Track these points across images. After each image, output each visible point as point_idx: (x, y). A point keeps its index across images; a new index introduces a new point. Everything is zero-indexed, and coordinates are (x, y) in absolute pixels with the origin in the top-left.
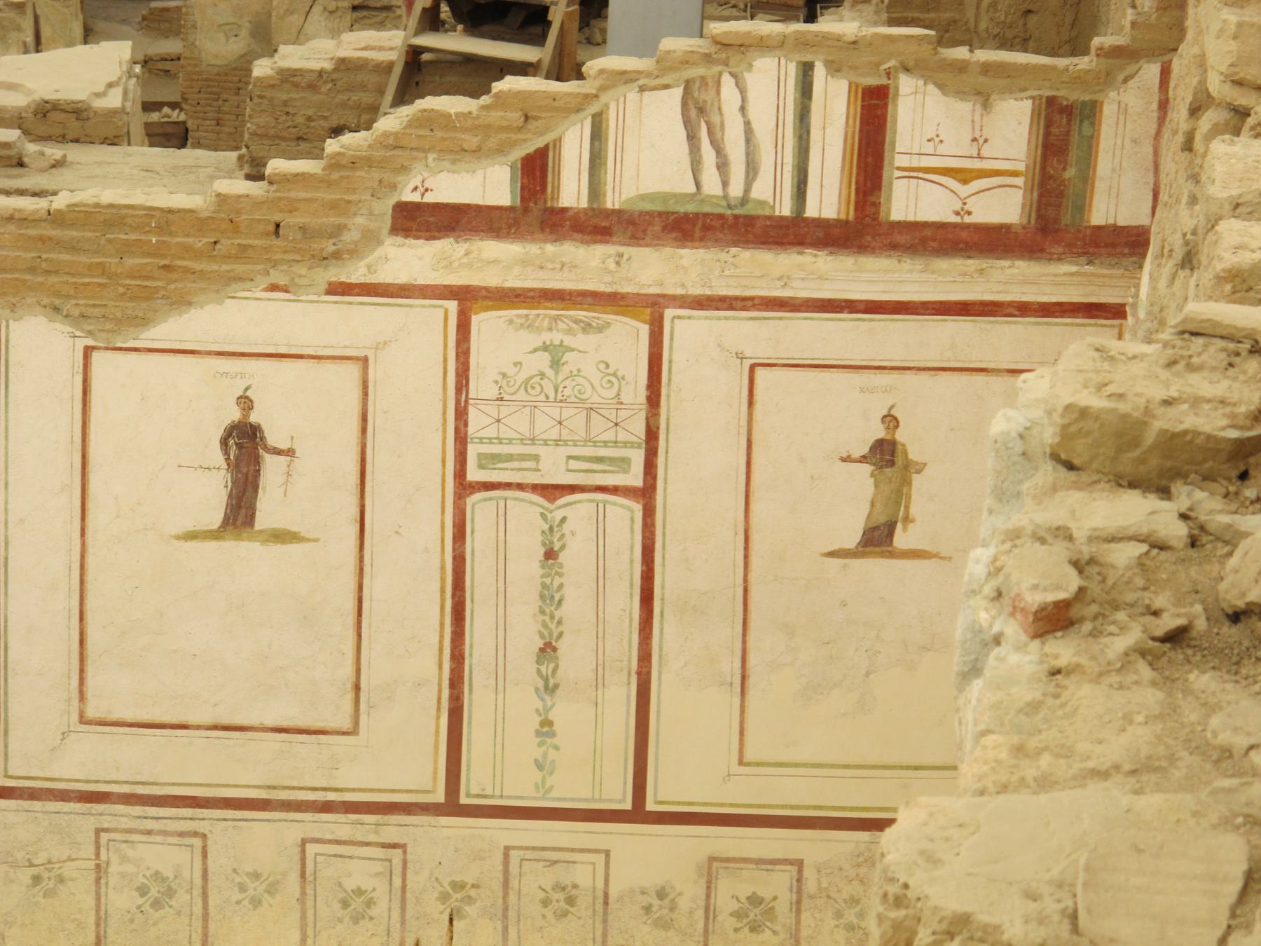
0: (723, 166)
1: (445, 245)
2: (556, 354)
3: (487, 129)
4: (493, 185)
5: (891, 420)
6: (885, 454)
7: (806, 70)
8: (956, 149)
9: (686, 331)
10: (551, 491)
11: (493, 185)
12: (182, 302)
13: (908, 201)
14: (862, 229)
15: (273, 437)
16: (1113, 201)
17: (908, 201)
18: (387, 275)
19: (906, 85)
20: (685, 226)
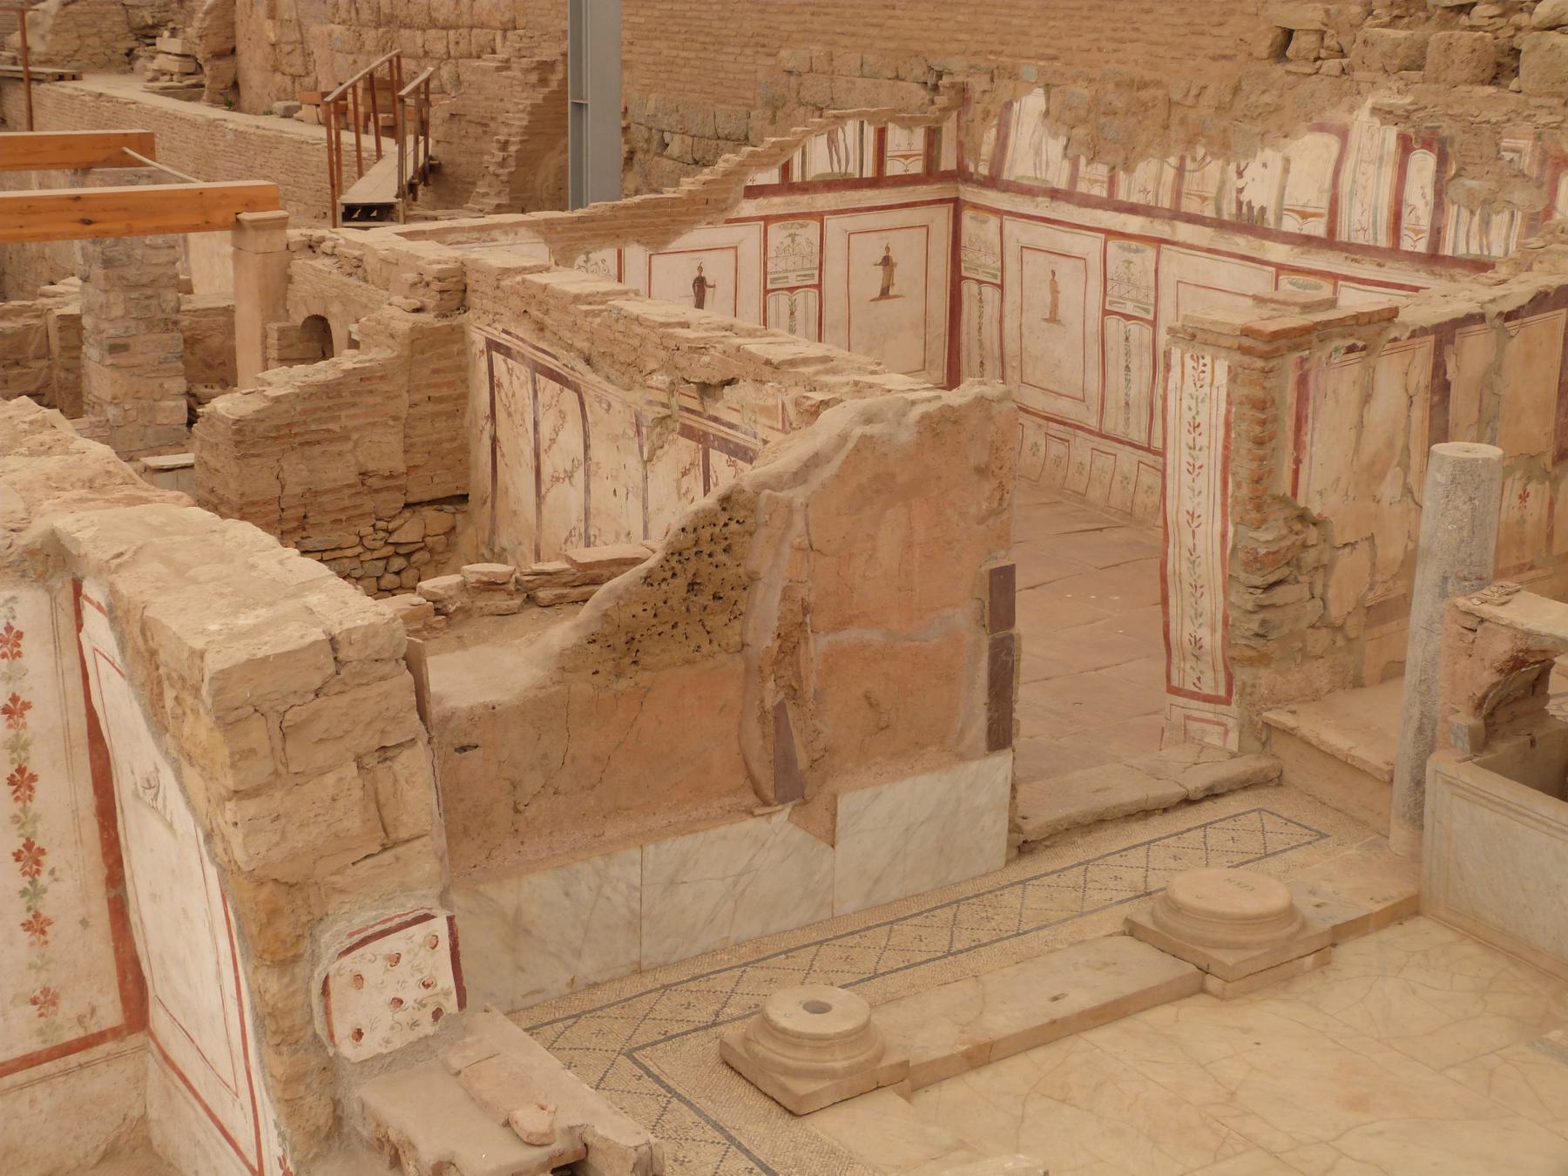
0: (839, 161)
1: (761, 201)
2: (793, 236)
3: (770, 156)
4: (771, 177)
5: (888, 249)
6: (887, 262)
7: (862, 123)
9: (832, 223)
10: (791, 289)
11: (771, 177)
13: (894, 168)
14: (879, 181)
15: (709, 282)
16: (948, 162)
17: (894, 168)
18: (744, 214)
19: (890, 126)
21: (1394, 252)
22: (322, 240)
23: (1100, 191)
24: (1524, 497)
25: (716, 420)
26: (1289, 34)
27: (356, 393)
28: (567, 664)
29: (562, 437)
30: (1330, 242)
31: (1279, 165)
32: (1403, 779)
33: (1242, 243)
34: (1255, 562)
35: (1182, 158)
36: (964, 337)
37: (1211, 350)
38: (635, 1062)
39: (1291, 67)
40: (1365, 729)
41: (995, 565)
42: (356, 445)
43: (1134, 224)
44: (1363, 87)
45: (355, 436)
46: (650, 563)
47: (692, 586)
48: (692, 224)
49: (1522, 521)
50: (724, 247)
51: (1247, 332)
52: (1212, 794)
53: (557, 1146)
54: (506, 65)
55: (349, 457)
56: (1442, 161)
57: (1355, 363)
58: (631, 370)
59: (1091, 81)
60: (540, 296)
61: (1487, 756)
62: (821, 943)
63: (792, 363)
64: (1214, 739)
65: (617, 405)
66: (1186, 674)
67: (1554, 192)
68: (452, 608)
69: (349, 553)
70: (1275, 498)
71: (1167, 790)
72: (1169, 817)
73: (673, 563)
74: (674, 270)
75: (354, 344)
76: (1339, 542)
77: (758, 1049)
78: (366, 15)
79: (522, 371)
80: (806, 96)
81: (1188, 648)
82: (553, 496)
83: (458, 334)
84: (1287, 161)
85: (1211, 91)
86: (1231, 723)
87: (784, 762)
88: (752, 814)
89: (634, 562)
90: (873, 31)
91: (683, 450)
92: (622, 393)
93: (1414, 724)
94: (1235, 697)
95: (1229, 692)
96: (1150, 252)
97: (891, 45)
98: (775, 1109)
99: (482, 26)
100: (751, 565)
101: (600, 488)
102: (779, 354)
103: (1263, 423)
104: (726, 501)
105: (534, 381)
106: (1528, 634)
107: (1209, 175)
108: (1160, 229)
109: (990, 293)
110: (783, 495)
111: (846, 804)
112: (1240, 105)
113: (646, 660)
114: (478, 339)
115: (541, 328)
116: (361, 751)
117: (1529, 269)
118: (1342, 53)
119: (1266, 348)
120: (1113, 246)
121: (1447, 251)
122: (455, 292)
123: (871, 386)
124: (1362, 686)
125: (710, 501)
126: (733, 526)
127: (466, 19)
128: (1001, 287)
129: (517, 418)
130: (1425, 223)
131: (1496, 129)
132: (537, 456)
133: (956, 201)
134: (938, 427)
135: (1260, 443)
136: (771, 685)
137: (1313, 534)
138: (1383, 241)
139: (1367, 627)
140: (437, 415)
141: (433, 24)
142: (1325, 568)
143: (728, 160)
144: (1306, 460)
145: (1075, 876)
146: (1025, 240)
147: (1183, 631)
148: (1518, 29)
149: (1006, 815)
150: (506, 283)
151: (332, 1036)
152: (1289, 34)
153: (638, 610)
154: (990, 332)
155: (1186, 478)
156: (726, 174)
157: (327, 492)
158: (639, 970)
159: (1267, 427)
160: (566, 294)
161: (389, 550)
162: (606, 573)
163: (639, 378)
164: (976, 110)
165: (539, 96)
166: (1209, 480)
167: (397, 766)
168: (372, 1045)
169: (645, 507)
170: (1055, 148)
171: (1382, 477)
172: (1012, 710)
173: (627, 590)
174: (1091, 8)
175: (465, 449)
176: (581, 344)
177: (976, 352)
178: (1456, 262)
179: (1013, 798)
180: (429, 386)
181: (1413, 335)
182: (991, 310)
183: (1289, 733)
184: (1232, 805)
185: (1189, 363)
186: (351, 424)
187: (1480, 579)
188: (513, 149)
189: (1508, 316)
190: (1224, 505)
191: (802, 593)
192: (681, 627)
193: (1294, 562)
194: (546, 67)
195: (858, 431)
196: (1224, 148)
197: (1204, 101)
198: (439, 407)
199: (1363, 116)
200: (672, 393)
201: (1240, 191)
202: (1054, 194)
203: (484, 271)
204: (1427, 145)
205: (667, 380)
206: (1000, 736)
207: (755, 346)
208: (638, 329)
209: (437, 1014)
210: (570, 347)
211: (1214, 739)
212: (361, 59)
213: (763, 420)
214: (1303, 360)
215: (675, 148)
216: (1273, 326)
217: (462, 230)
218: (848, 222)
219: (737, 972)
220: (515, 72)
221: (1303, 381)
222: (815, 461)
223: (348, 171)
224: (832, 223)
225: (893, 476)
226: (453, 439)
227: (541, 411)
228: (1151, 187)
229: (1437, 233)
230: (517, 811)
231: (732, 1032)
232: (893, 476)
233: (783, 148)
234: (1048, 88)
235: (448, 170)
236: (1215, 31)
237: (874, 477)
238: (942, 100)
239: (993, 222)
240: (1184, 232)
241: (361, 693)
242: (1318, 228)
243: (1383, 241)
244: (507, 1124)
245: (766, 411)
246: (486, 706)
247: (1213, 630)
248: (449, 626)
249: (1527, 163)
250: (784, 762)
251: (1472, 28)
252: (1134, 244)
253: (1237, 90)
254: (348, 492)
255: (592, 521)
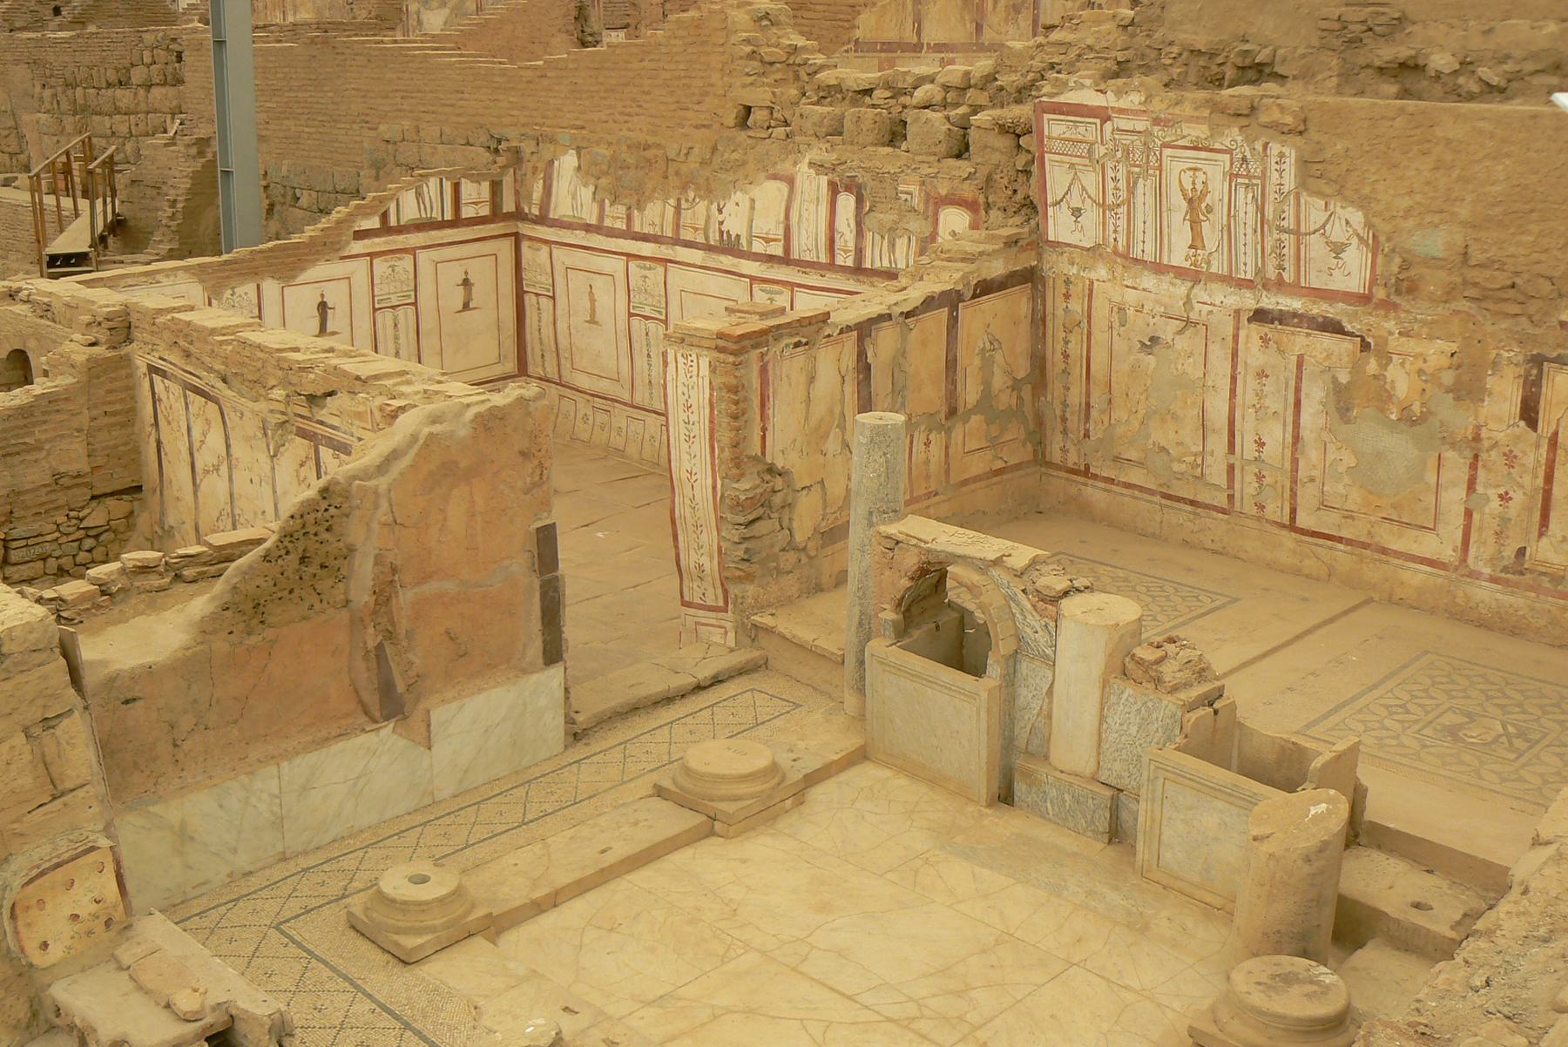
4: (373, 223)
6: (466, 283)
8: (474, 197)
9: (422, 256)
11: (373, 223)
12: (304, 269)
13: (467, 212)
14: (457, 222)
16: (508, 206)
17: (467, 212)
20: (419, 226)
21: (831, 266)
22: (19, 290)
23: (621, 225)
24: (927, 444)
25: (322, 423)
26: (748, 109)
27: (44, 413)
28: (206, 629)
29: (209, 439)
30: (786, 260)
31: (747, 204)
32: (851, 661)
33: (727, 261)
34: (738, 506)
35: (679, 200)
36: (528, 337)
37: (697, 350)
38: (282, 933)
39: (751, 133)
40: (824, 623)
41: (540, 524)
42: (49, 454)
43: (647, 249)
44: (802, 147)
45: (47, 447)
46: (267, 545)
47: (303, 560)
48: (314, 262)
49: (927, 461)
50: (340, 279)
51: (721, 336)
52: (717, 681)
53: (209, 1020)
54: (172, 142)
55: (44, 463)
56: (860, 201)
57: (800, 359)
58: (258, 387)
59: (610, 144)
60: (186, 331)
61: (906, 641)
62: (425, 824)
63: (376, 377)
64: (717, 638)
65: (248, 412)
66: (694, 592)
67: (936, 222)
68: (114, 589)
69: (49, 538)
70: (749, 457)
71: (687, 681)
72: (685, 701)
73: (286, 543)
74: (302, 297)
75: (46, 374)
76: (799, 486)
77: (375, 915)
78: (65, 106)
79: (176, 389)
80: (400, 158)
81: (695, 572)
82: (204, 487)
83: (126, 361)
84: (753, 201)
85: (696, 151)
86: (729, 625)
87: (386, 688)
88: (363, 730)
89: (259, 542)
90: (448, 110)
91: (300, 447)
92: (250, 404)
93: (856, 620)
94: (730, 607)
95: (726, 602)
96: (660, 269)
97: (462, 120)
98: (393, 961)
99: (156, 111)
100: (350, 540)
101: (240, 477)
102: (364, 371)
103: (737, 403)
104: (325, 492)
105: (185, 397)
106: (929, 551)
107: (698, 212)
108: (665, 251)
109: (543, 300)
110: (371, 483)
111: (437, 716)
112: (717, 160)
113: (271, 619)
114: (141, 365)
115: (188, 355)
116: (28, 723)
117: (921, 279)
118: (786, 123)
119: (735, 347)
120: (632, 265)
121: (868, 265)
122: (122, 328)
123: (437, 393)
124: (822, 590)
125: (312, 493)
126: (332, 511)
127: (143, 107)
128: (553, 298)
129: (174, 424)
130: (851, 245)
131: (895, 177)
132: (191, 454)
133: (517, 238)
134: (489, 422)
135: (735, 417)
136: (371, 630)
137: (779, 483)
138: (823, 259)
139: (823, 547)
140: (113, 425)
141: (117, 111)
142: (788, 506)
143: (340, 212)
144: (770, 428)
145: (617, 755)
146: (568, 263)
147: (690, 559)
148: (904, 107)
149: (562, 712)
150: (160, 320)
151: (22, 950)
152: (748, 109)
153: (260, 581)
154: (547, 332)
155: (685, 446)
156: (339, 222)
157: (27, 491)
158: (284, 859)
159: (740, 406)
160: (205, 328)
161: (81, 533)
162: (237, 552)
163: (262, 391)
164: (527, 167)
165: (198, 164)
166: (701, 447)
167: (58, 732)
168: (56, 953)
169: (275, 492)
170: (586, 194)
171: (826, 436)
172: (561, 632)
173: (250, 567)
174: (606, 91)
175: (137, 450)
176: (218, 367)
177: (537, 347)
178: (874, 273)
179: (567, 698)
180: (105, 403)
181: (841, 332)
182: (547, 317)
183: (770, 631)
184: (730, 688)
185: (681, 360)
186: (43, 437)
187: (895, 511)
188: (180, 205)
189: (908, 315)
190: (713, 464)
191: (390, 558)
192: (296, 592)
193: (766, 504)
194: (203, 143)
195: (426, 430)
196: (708, 192)
197: (691, 158)
198: (113, 420)
199: (803, 167)
200: (288, 403)
201: (721, 223)
202: (588, 228)
203: (143, 312)
204: (848, 189)
205: (283, 393)
206: (553, 653)
207: (349, 366)
208: (261, 355)
209: (108, 923)
210: (210, 370)
211: (717, 638)
212: (63, 139)
213: (357, 422)
214: (763, 355)
215: (304, 202)
216: (739, 331)
217: (133, 275)
218: (435, 254)
219: (360, 854)
220: (180, 148)
221: (764, 370)
222: (394, 455)
223: (51, 228)
224: (422, 256)
225: (456, 463)
226: (127, 444)
227: (192, 419)
228: (657, 221)
229: (859, 252)
230: (175, 745)
231: (357, 903)
232: (456, 463)
233: (381, 201)
234: (578, 149)
235: (132, 223)
236: (696, 107)
237: (442, 466)
238: (501, 160)
239: (545, 249)
240: (683, 254)
241: (22, 678)
242: (777, 249)
243: (823, 259)
244: (168, 1006)
245: (359, 415)
246: (142, 666)
247: (711, 558)
248: (113, 603)
249: (917, 202)
250: (386, 688)
251: (874, 106)
252: (648, 264)
253: (714, 150)
254: (44, 490)
255: (236, 503)
